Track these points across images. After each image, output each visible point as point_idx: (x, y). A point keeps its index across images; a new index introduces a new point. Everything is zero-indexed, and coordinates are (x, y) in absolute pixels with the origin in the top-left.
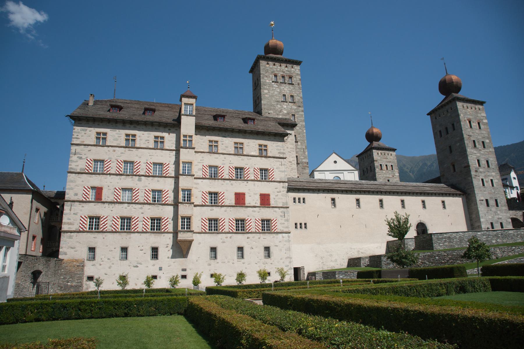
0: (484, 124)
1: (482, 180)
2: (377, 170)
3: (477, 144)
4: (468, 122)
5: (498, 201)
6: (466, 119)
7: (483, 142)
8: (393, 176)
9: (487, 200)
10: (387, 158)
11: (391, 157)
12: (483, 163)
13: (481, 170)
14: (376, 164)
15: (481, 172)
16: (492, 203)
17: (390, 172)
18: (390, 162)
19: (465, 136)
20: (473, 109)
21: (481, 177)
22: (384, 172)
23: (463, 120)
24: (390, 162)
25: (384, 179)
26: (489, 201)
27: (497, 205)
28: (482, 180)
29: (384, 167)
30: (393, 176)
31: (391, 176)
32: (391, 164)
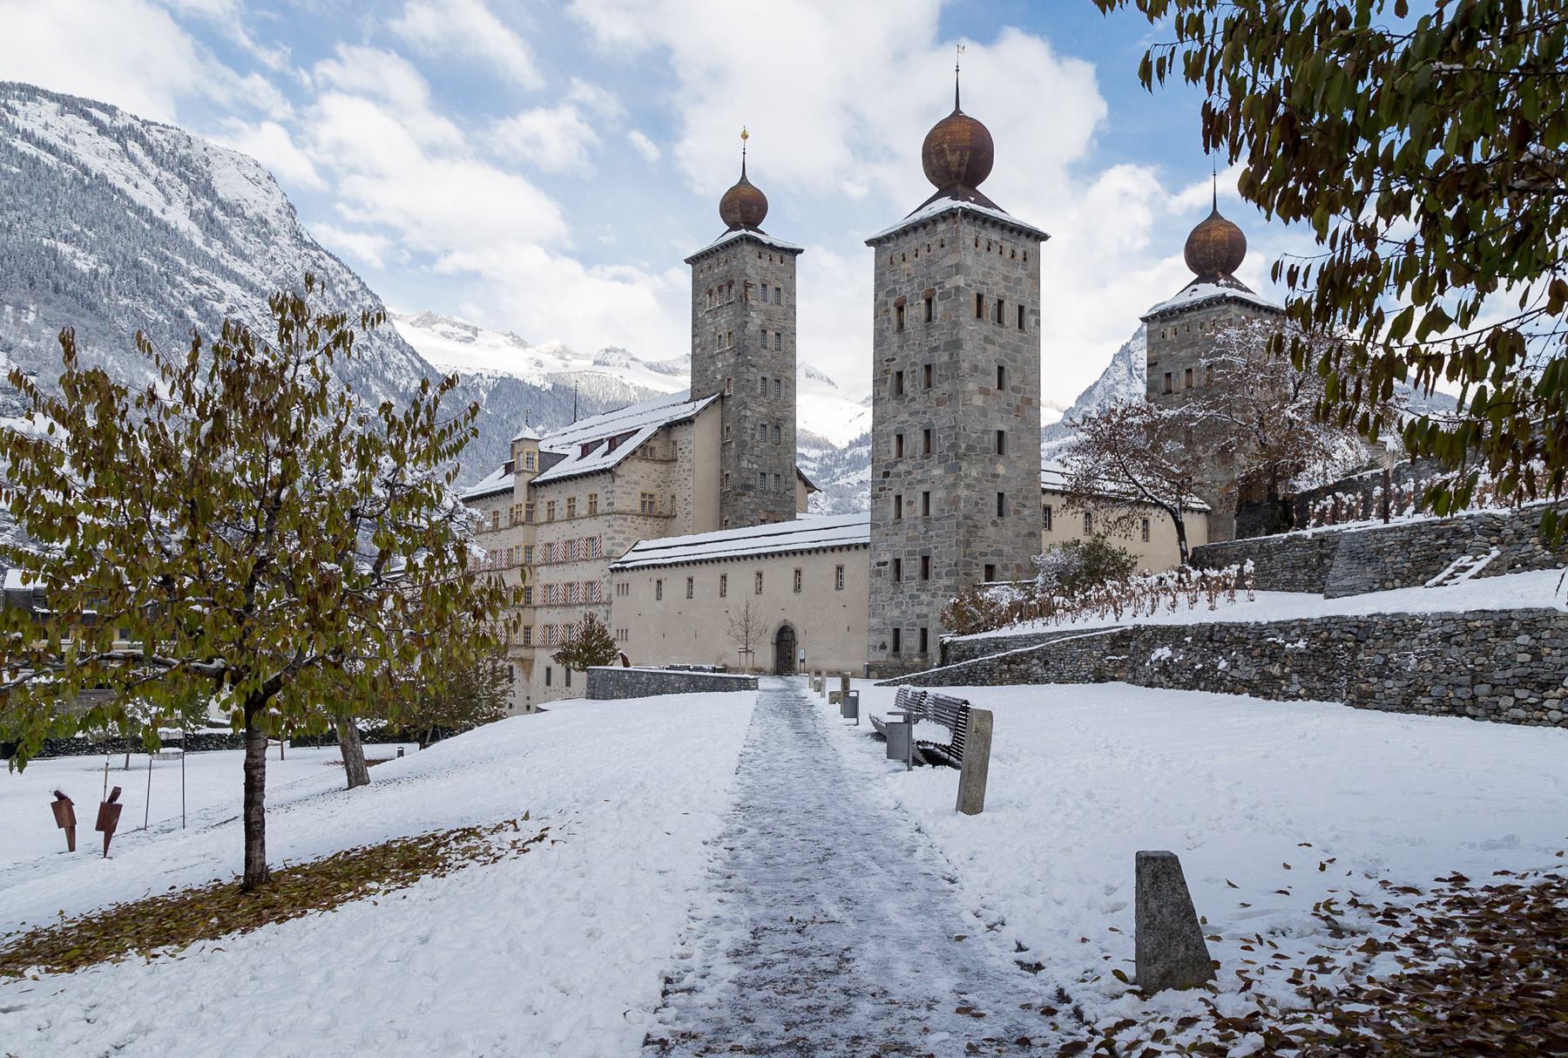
1: (899, 498)
3: (906, 384)
4: (893, 310)
5: (933, 562)
6: (892, 301)
7: (928, 368)
9: (898, 561)
12: (915, 440)
13: (901, 467)
15: (899, 475)
16: (911, 568)
20: (923, 253)
21: (895, 491)
26: (903, 562)
27: (925, 575)
28: (899, 498)
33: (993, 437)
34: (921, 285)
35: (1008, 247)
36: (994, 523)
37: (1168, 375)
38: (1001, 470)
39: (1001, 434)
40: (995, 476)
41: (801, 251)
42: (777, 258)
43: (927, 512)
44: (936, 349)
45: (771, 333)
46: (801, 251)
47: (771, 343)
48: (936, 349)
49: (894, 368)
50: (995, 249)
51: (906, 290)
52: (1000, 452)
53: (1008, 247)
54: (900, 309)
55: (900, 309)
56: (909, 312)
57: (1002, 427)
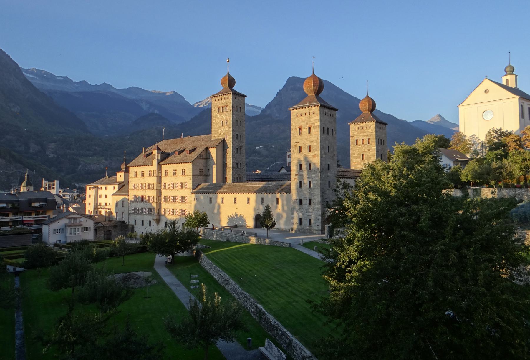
0: (315, 127)
2: (352, 146)
3: (302, 150)
4: (298, 129)
6: (297, 127)
8: (369, 150)
10: (364, 132)
11: (370, 130)
14: (352, 140)
17: (365, 146)
18: (367, 136)
19: (292, 144)
22: (359, 147)
23: (294, 129)
24: (367, 136)
25: (359, 154)
29: (360, 142)
30: (369, 150)
31: (366, 150)
32: (368, 138)
33: (327, 165)
34: (307, 123)
35: (329, 113)
36: (328, 190)
37: (356, 140)
38: (329, 174)
39: (329, 164)
40: (328, 176)
41: (246, 96)
42: (240, 99)
43: (310, 186)
44: (312, 142)
45: (239, 121)
46: (246, 96)
47: (239, 124)
48: (312, 142)
49: (299, 145)
50: (327, 114)
51: (302, 124)
52: (329, 169)
53: (329, 113)
54: (300, 129)
55: (300, 129)
56: (303, 130)
57: (329, 163)
